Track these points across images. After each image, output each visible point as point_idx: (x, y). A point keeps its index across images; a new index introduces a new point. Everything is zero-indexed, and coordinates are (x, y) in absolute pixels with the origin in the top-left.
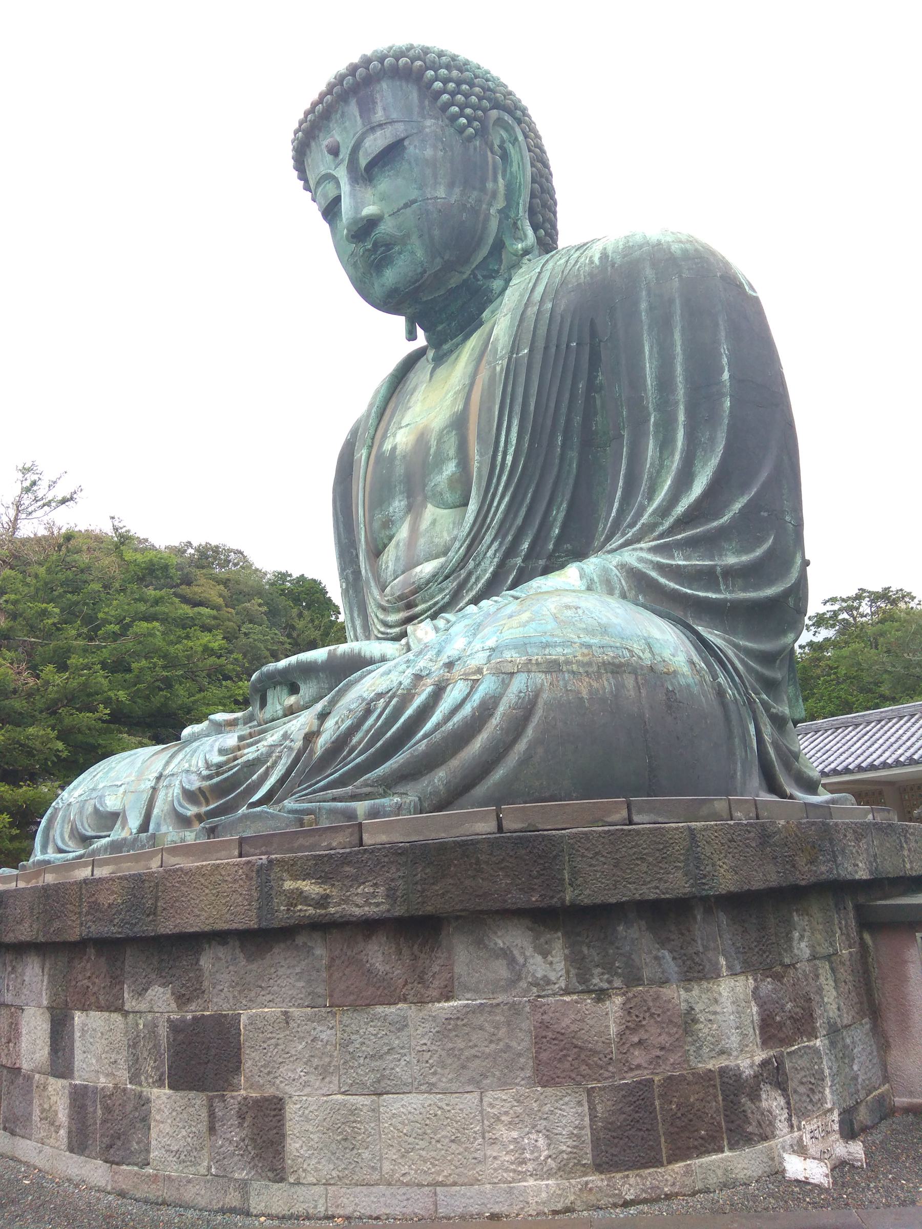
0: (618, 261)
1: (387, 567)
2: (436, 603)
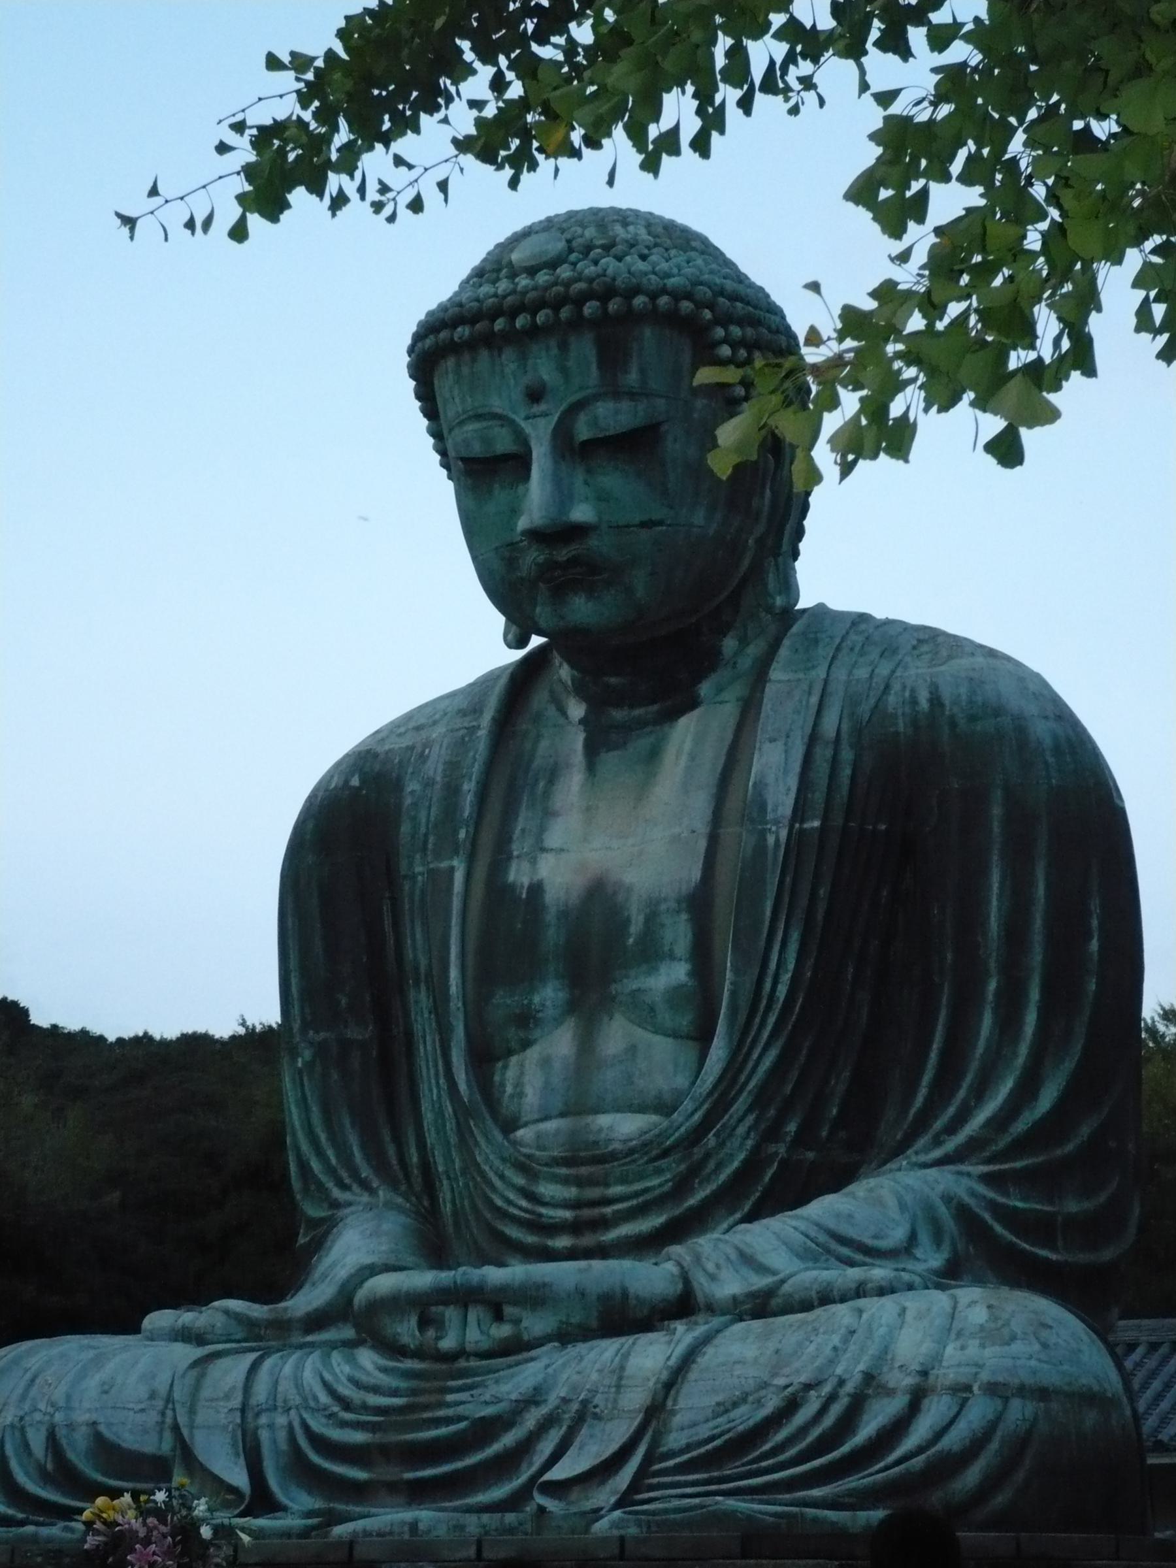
0: (962, 722)
1: (521, 1095)
2: (646, 1190)
